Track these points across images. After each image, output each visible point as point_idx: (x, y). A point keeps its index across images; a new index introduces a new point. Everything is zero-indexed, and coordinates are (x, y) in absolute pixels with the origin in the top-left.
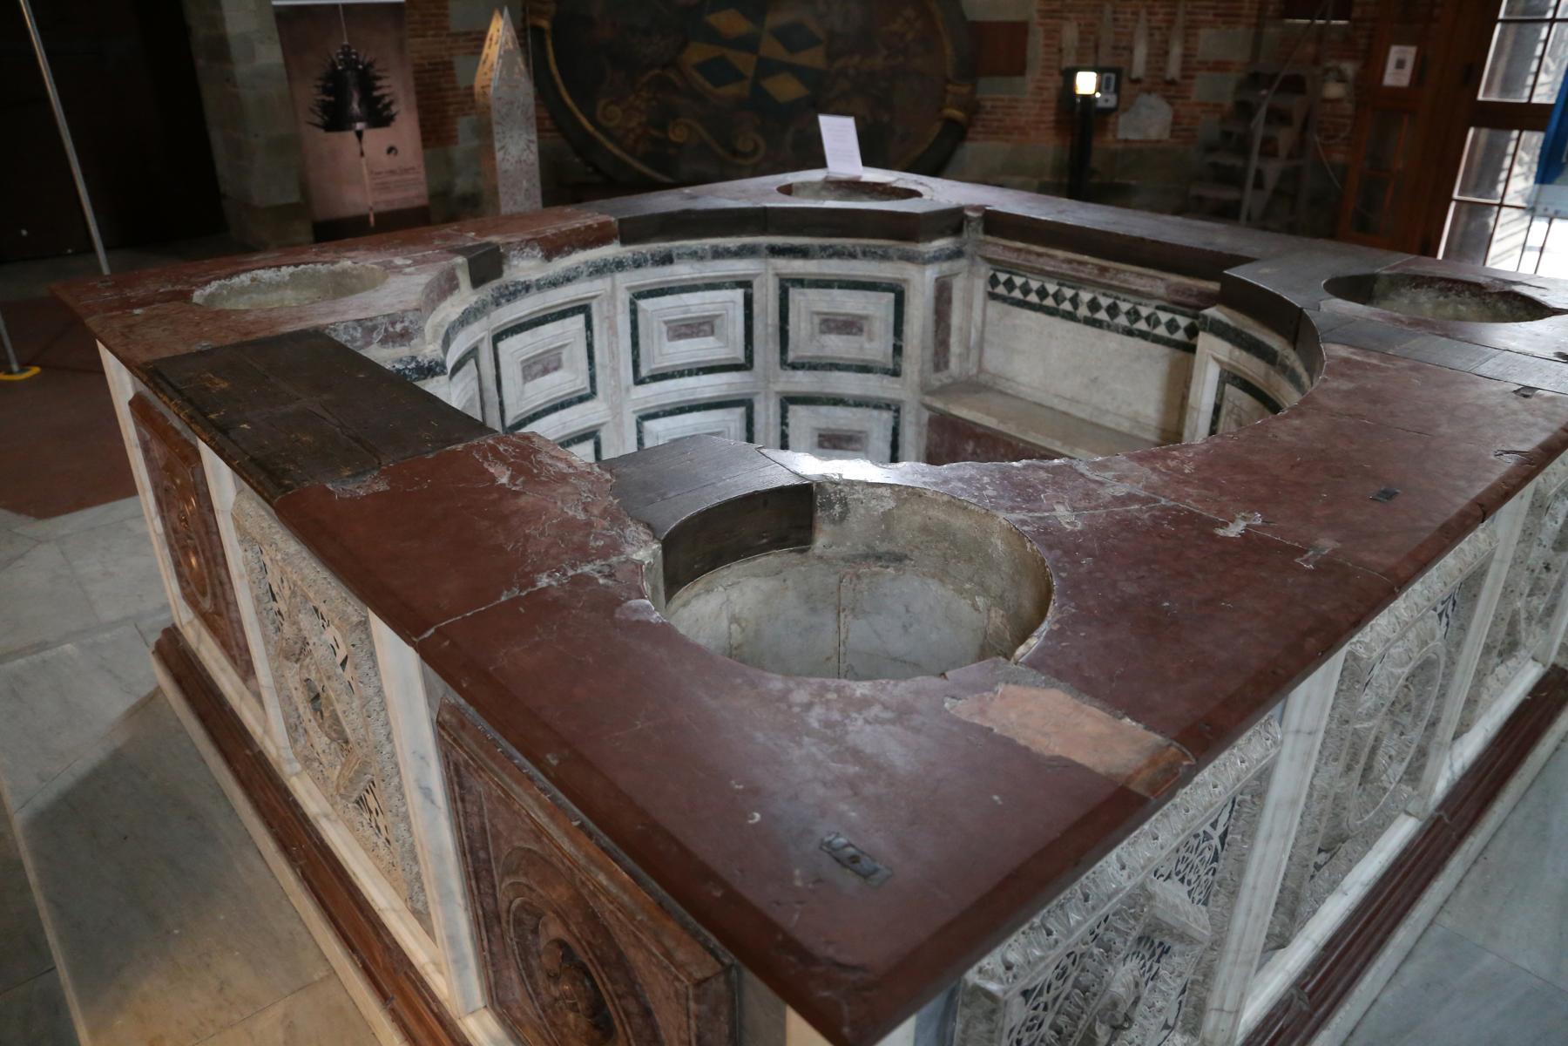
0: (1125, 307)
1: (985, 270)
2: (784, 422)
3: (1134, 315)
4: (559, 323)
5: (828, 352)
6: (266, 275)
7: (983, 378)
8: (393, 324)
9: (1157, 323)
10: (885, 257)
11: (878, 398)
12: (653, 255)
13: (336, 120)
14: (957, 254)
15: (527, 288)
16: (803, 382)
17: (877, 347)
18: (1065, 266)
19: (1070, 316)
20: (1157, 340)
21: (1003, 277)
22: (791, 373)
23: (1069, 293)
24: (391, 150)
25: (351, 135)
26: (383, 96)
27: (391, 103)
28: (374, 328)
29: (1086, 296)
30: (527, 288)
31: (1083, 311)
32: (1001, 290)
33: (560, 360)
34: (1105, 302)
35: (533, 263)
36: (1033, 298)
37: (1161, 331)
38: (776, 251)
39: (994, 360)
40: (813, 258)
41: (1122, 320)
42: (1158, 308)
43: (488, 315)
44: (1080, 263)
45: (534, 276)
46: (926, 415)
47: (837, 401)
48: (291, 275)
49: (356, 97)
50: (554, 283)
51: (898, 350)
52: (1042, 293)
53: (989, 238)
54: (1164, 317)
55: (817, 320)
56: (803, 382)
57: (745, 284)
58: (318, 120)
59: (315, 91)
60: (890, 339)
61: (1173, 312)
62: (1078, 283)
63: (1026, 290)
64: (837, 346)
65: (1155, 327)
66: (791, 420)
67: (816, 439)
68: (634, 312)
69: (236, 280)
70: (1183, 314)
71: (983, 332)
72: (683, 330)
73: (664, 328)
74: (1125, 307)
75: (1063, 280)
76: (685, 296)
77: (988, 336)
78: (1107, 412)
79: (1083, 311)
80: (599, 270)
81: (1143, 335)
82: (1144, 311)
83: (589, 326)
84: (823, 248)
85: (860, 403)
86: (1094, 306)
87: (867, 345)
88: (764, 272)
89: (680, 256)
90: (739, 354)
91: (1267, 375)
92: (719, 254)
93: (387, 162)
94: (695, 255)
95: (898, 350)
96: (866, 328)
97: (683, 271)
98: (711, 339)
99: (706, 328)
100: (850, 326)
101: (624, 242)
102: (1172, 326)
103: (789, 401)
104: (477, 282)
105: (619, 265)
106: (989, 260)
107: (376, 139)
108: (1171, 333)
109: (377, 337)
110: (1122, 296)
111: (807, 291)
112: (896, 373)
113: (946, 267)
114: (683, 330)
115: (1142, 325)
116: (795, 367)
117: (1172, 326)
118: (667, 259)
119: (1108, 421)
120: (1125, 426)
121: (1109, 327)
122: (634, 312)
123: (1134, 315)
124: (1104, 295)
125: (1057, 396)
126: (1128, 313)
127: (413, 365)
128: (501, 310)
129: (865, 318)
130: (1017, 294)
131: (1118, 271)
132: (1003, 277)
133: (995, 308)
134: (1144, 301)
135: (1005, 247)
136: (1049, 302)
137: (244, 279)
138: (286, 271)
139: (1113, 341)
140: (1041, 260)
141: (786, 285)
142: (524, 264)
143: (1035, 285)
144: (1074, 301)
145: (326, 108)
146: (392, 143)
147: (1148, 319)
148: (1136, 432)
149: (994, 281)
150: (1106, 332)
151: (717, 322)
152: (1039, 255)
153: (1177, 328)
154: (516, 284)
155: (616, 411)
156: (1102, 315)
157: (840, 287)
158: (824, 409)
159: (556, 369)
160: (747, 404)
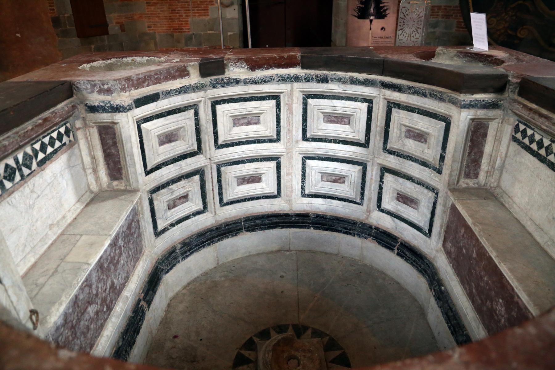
1: (513, 120)
2: (381, 181)
4: (259, 102)
5: (406, 149)
6: (138, 59)
8: (103, 85)
10: (441, 99)
12: (316, 77)
13: (363, 14)
14: (494, 106)
15: (237, 82)
16: (392, 162)
17: (431, 153)
21: (522, 127)
24: (383, 28)
25: (368, 21)
26: (384, 6)
27: (387, 9)
28: (95, 85)
30: (237, 82)
32: (519, 136)
33: (259, 120)
35: (242, 70)
36: (534, 146)
39: (506, 182)
40: (404, 93)
43: (206, 91)
45: (243, 77)
47: (409, 178)
48: (147, 60)
49: (373, 6)
50: (256, 82)
51: (442, 158)
55: (404, 129)
56: (392, 162)
57: (369, 101)
58: (356, 14)
59: (357, 3)
64: (411, 146)
67: (395, 195)
68: (305, 104)
69: (125, 59)
72: (333, 119)
73: (322, 116)
76: (335, 101)
80: (284, 79)
83: (278, 106)
84: (410, 88)
85: (420, 183)
87: (426, 151)
89: (333, 80)
92: (354, 82)
93: (380, 33)
94: (340, 80)
95: (442, 158)
97: (333, 87)
98: (348, 126)
99: (346, 120)
100: (420, 137)
101: (303, 68)
104: (204, 73)
105: (297, 79)
107: (377, 24)
109: (96, 89)
111: (401, 111)
112: (439, 172)
113: (481, 113)
114: (333, 119)
116: (390, 152)
118: (325, 80)
122: (305, 104)
125: (531, 219)
127: (109, 105)
128: (215, 90)
135: (525, 106)
137: (129, 59)
138: (145, 58)
142: (237, 70)
143: (537, 137)
145: (360, 9)
146: (383, 26)
154: (229, 79)
155: (289, 151)
158: (401, 180)
159: (256, 124)
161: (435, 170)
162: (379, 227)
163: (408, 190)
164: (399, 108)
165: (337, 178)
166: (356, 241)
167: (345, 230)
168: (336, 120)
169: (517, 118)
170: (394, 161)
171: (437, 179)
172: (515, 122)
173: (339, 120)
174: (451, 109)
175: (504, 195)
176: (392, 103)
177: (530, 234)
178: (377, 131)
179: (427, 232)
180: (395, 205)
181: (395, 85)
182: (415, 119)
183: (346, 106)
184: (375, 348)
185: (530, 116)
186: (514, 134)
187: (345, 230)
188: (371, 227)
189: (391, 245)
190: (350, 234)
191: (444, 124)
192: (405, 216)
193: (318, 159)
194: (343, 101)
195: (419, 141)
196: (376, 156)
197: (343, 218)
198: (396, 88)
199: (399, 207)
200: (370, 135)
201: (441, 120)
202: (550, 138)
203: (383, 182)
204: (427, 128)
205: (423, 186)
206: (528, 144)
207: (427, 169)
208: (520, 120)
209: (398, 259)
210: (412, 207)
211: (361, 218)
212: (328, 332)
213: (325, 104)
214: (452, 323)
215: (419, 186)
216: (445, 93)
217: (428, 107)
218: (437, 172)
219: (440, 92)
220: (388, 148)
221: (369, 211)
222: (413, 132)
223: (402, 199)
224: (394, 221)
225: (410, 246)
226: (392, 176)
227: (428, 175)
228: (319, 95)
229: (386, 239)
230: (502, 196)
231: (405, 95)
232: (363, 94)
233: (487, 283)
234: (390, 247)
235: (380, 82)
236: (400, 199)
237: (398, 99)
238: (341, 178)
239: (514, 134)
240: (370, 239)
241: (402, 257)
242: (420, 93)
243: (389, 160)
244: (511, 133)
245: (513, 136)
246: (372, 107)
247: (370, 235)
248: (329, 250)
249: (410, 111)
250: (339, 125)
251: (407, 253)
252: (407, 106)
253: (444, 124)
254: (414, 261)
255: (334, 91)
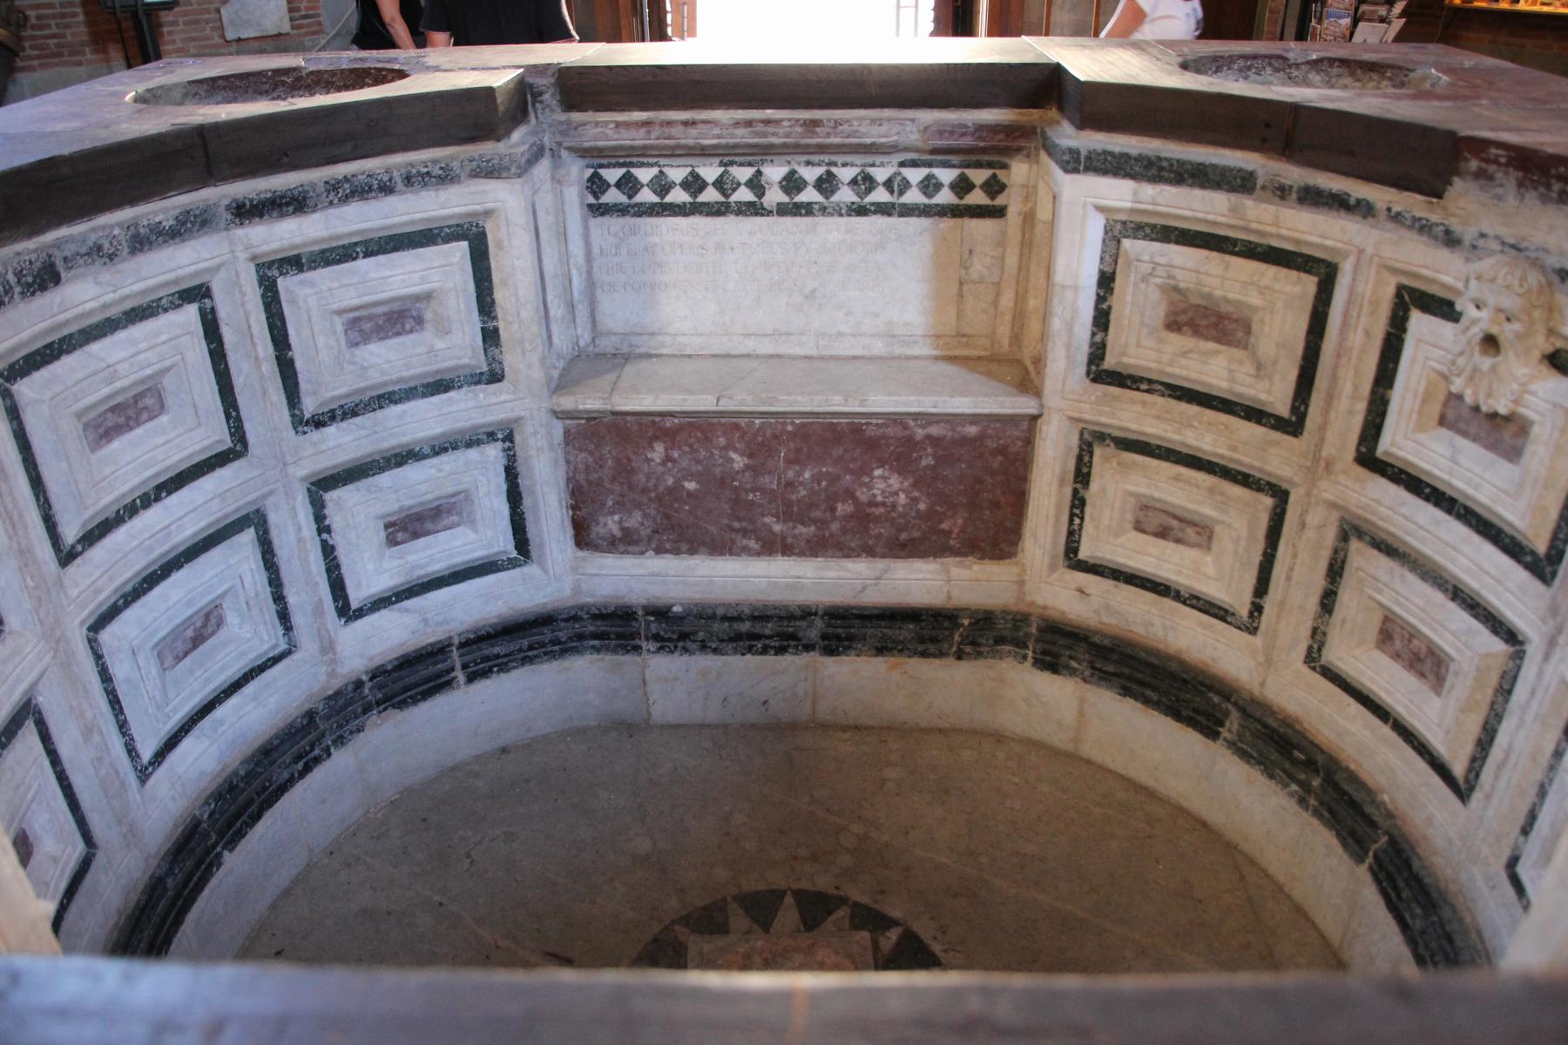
0: (845, 174)
1: (577, 171)
2: (323, 528)
3: (865, 182)
5: (374, 378)
7: (606, 344)
9: (905, 185)
10: (446, 177)
11: (477, 427)
12: (19, 274)
18: (741, 131)
19: (753, 209)
20: (908, 211)
21: (612, 175)
22: (315, 435)
23: (743, 174)
29: (774, 173)
31: (774, 196)
32: (613, 196)
34: (810, 174)
36: (678, 196)
37: (914, 197)
38: (245, 212)
39: (617, 312)
40: (315, 209)
41: (846, 195)
42: (902, 164)
44: (767, 122)
46: (558, 428)
51: (491, 337)
52: (694, 184)
53: (577, 116)
54: (915, 175)
55: (339, 324)
57: (198, 293)
60: (475, 322)
61: (930, 165)
62: (763, 152)
63: (662, 186)
64: (389, 359)
65: (901, 193)
66: (335, 518)
67: (383, 534)
70: (946, 165)
71: (589, 273)
74: (845, 174)
75: (727, 154)
76: (95, 347)
77: (599, 275)
78: (840, 334)
79: (774, 196)
81: (884, 210)
82: (881, 175)
84: (333, 186)
85: (442, 447)
86: (792, 184)
87: (440, 345)
88: (224, 256)
90: (216, 435)
91: (1234, 210)
92: (141, 242)
94: (100, 254)
95: (491, 337)
96: (428, 315)
97: (83, 295)
99: (149, 401)
100: (398, 318)
102: (930, 186)
103: (323, 484)
106: (583, 153)
108: (930, 196)
110: (840, 159)
112: (495, 377)
114: (111, 420)
115: (880, 195)
116: (318, 423)
117: (930, 186)
119: (845, 348)
120: (878, 347)
121: (824, 210)
123: (865, 182)
124: (808, 163)
126: (854, 182)
129: (427, 297)
130: (647, 196)
131: (838, 123)
132: (612, 175)
133: (606, 228)
134: (878, 159)
135: (618, 125)
136: (710, 195)
139: (832, 231)
140: (693, 131)
141: (272, 273)
143: (677, 174)
144: (756, 184)
147: (888, 185)
148: (897, 351)
149: (596, 185)
150: (820, 220)
151: (168, 382)
152: (686, 123)
153: (938, 186)
156: (809, 195)
157: (367, 255)
158: (385, 479)
160: (255, 520)
161: (478, 383)
162: (377, 662)
163: (423, 488)
164: (301, 270)
165: (199, 624)
166: (340, 764)
167: (300, 766)
168: (121, 420)
169: (581, 162)
170: (348, 438)
171: (503, 397)
172: (582, 172)
173: (131, 412)
174: (485, 192)
175: (635, 340)
176: (270, 264)
177: (772, 356)
178: (262, 378)
179: (514, 554)
180: (396, 562)
181: (282, 197)
182: (374, 275)
183: (143, 345)
184: (728, 834)
185: (653, 136)
186: (591, 200)
187: (300, 766)
188: (359, 684)
189: (438, 676)
190: (317, 760)
191: (465, 244)
192: (439, 566)
193: (127, 604)
194: (121, 335)
195: (398, 334)
196: (289, 459)
197: (276, 736)
198: (288, 204)
199: (410, 558)
200: (237, 409)
201: (448, 239)
202: (717, 160)
203: (328, 530)
204: (423, 280)
205: (455, 448)
206: (656, 199)
207: (452, 394)
208: (596, 161)
209: (483, 687)
210: (446, 529)
211: (316, 688)
212: (657, 928)
213: (80, 376)
214: (767, 632)
215: (444, 458)
216: (453, 158)
217: (405, 218)
218: (489, 382)
219: (435, 162)
220: (307, 416)
221: (328, 647)
222: (370, 318)
223: (404, 529)
224: (407, 610)
225: (492, 625)
226: (350, 487)
227: (472, 404)
228: (38, 352)
229: (413, 677)
230: (631, 346)
231: (316, 216)
232: (182, 272)
233: (816, 479)
234: (439, 684)
235: (228, 208)
236: (400, 536)
237: (298, 240)
238: (208, 616)
239: (591, 200)
240: (374, 717)
241: (486, 674)
242: (370, 189)
243: (331, 444)
244: (582, 203)
245: (590, 206)
246: (213, 310)
247: (367, 709)
248: (282, 879)
249: (339, 262)
250: (139, 431)
251: (496, 650)
252: (323, 251)
253: (465, 244)
254: (531, 648)
255: (88, 306)
